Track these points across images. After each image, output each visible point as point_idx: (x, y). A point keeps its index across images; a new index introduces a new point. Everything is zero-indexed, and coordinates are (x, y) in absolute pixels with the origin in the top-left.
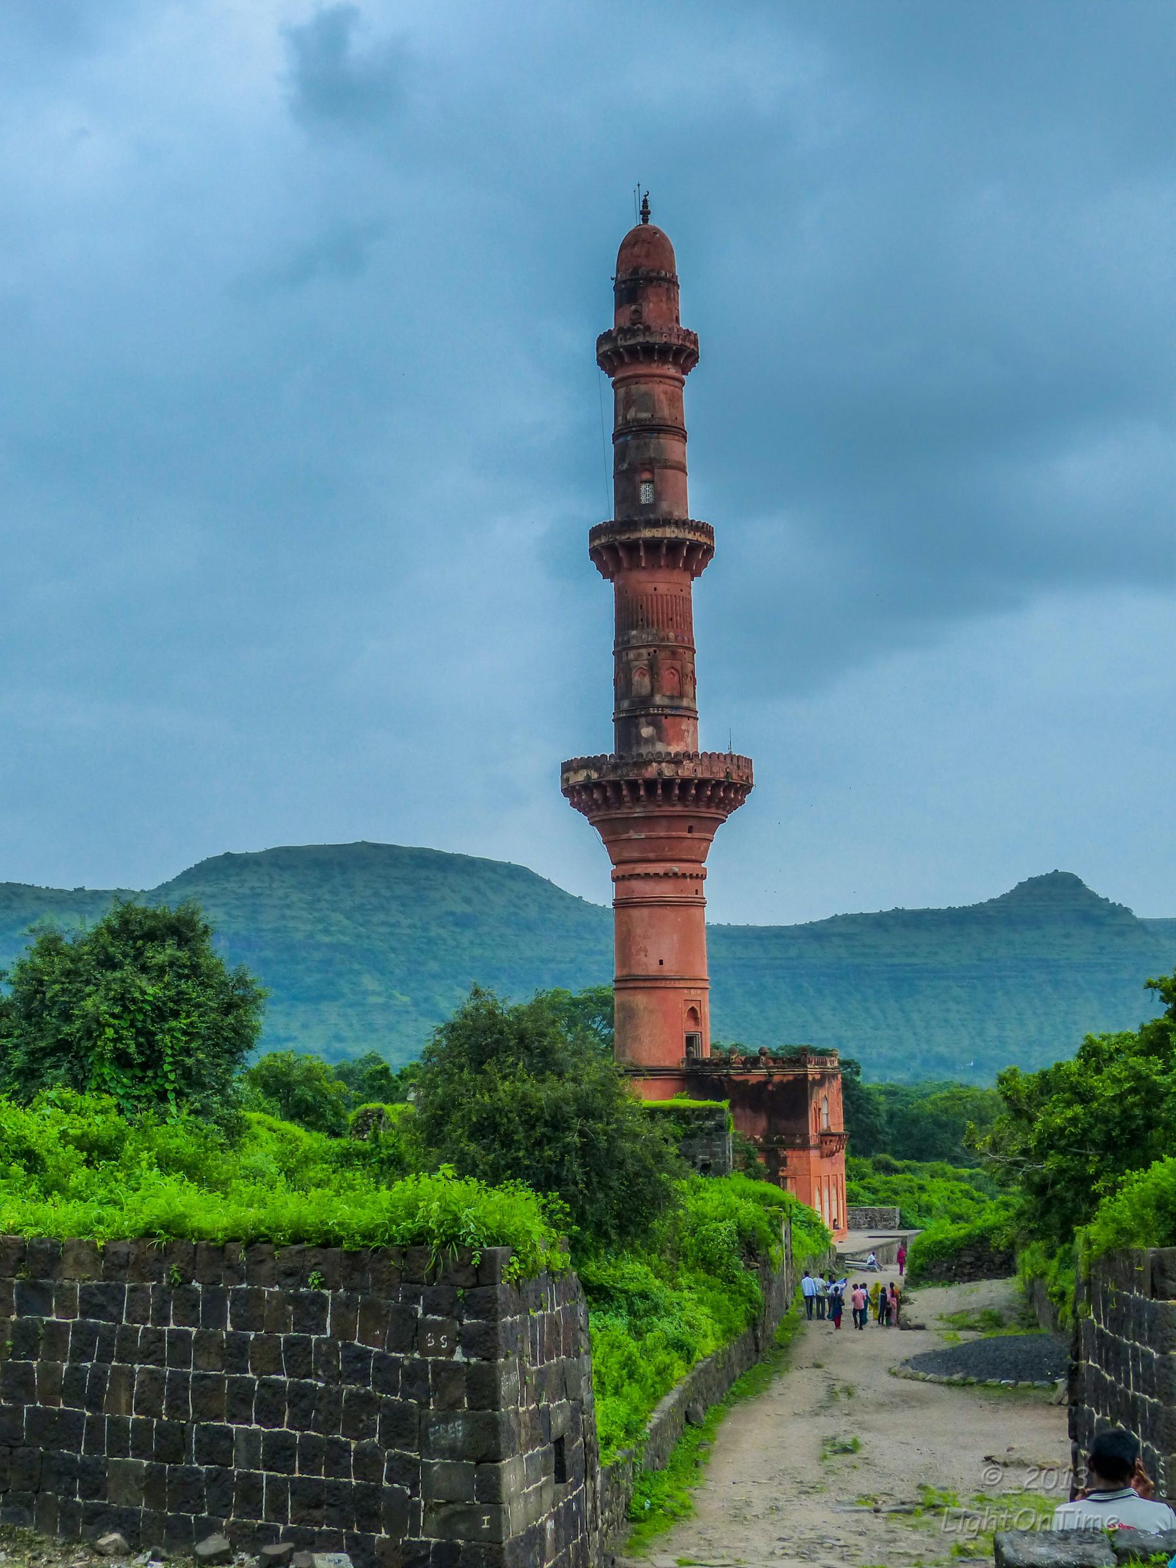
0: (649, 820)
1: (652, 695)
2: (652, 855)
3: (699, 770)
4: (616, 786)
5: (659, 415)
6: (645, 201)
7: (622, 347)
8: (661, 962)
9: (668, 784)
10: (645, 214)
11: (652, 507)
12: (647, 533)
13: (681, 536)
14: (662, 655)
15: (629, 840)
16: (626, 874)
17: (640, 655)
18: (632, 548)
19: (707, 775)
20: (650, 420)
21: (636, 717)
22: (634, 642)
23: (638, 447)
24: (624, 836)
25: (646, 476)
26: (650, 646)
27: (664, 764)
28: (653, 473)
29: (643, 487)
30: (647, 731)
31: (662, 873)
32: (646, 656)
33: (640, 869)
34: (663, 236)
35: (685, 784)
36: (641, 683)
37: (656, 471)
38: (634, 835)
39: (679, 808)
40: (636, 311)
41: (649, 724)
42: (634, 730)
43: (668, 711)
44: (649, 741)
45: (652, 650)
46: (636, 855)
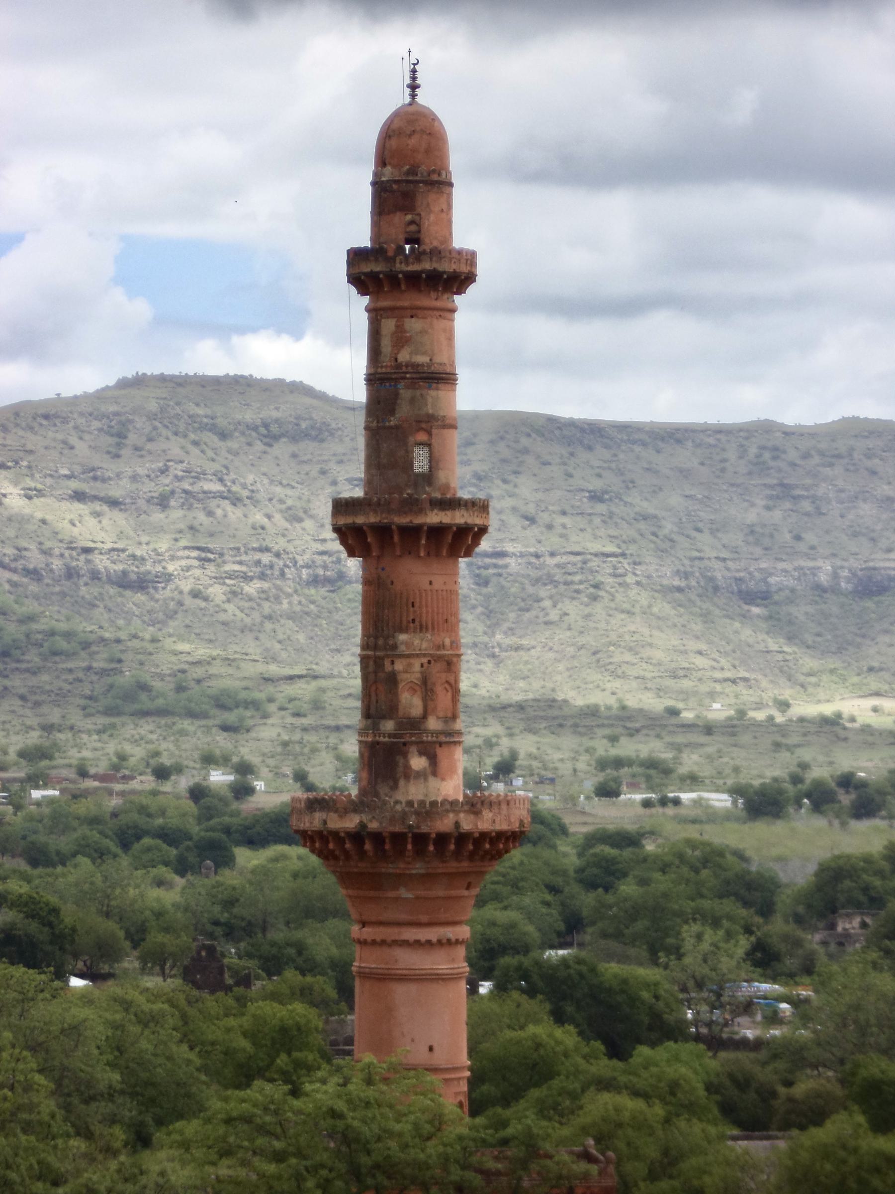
0: (429, 878)
1: (425, 717)
2: (424, 918)
3: (498, 820)
4: (398, 838)
5: (437, 359)
6: (414, 71)
7: (401, 272)
8: (431, 1049)
9: (462, 838)
10: (414, 87)
11: (428, 478)
12: (434, 518)
13: (470, 521)
14: (436, 668)
15: (397, 899)
16: (378, 939)
17: (410, 665)
18: (411, 533)
19: (504, 827)
20: (429, 366)
21: (405, 744)
22: (402, 648)
23: (412, 401)
24: (391, 894)
25: (422, 437)
26: (424, 655)
27: (462, 815)
28: (430, 434)
29: (416, 450)
30: (418, 763)
31: (434, 940)
32: (417, 667)
33: (411, 934)
34: (434, 118)
35: (484, 835)
36: (411, 703)
37: (434, 431)
38: (404, 893)
39: (465, 864)
40: (412, 222)
41: (421, 753)
42: (401, 760)
43: (443, 739)
44: (421, 775)
45: (424, 660)
46: (403, 917)
